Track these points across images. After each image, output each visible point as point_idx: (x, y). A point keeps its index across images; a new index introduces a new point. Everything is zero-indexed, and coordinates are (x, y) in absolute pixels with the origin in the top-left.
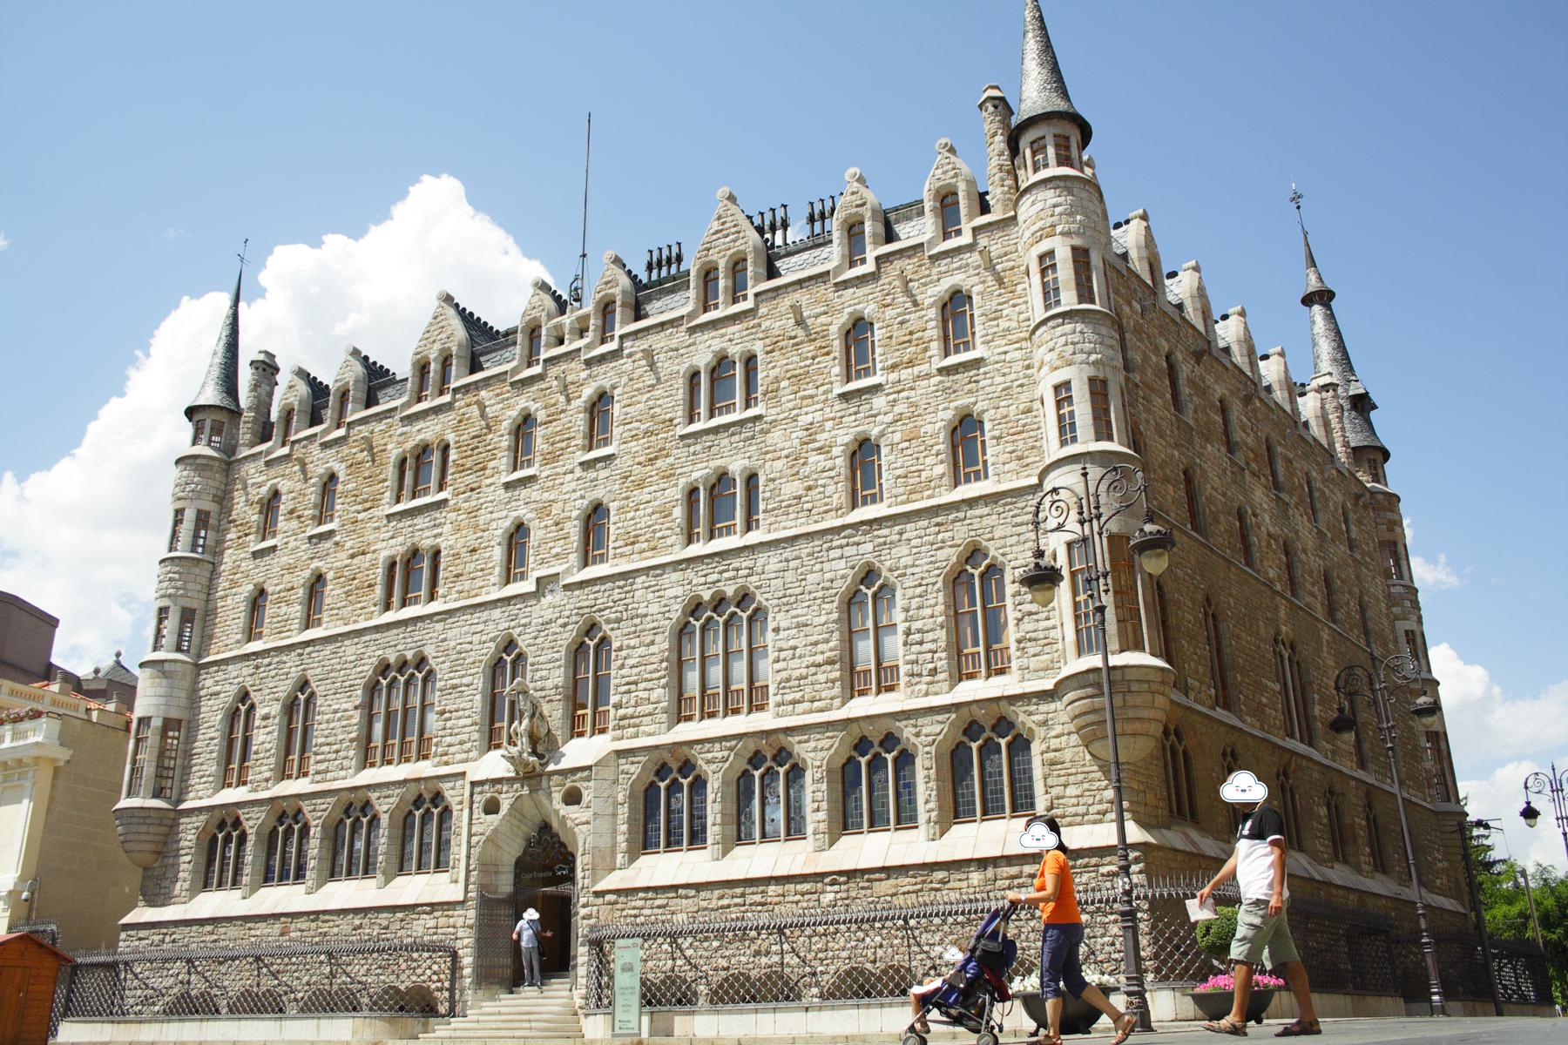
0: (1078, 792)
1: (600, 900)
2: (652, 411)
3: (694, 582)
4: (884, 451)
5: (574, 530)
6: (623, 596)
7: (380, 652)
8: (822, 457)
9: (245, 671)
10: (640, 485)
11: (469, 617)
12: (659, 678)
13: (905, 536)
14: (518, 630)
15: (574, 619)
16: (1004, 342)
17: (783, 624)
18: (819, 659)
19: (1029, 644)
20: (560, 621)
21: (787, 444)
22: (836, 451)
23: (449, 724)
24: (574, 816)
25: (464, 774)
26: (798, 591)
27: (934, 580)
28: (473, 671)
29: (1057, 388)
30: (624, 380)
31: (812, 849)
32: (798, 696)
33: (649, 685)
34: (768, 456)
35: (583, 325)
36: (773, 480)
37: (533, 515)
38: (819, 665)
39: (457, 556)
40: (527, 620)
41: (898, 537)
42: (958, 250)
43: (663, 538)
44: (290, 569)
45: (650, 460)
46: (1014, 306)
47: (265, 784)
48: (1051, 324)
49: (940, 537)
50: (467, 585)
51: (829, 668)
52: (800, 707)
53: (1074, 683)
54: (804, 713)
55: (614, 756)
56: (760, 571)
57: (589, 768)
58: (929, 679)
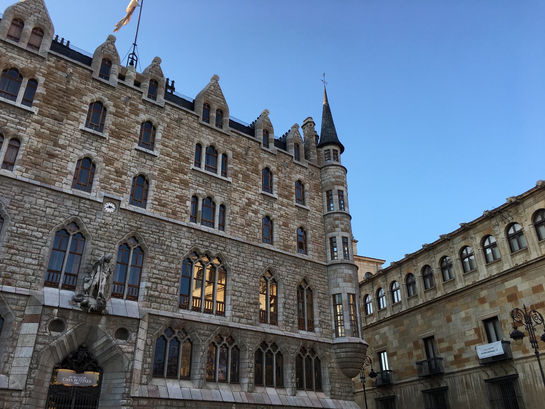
0: (339, 387)
1: (136, 403)
2: (179, 149)
3: (197, 241)
4: (276, 226)
5: (129, 180)
6: (158, 231)
8: (253, 215)
10: (169, 179)
11: (45, 195)
12: (175, 282)
13: (285, 264)
14: (85, 220)
15: (127, 230)
16: (315, 209)
17: (237, 280)
18: (252, 301)
19: (323, 323)
20: (116, 227)
21: (240, 202)
22: (260, 216)
23: (14, 258)
24: (124, 347)
25: (29, 296)
26: (243, 267)
27: (293, 285)
28: (43, 230)
29: (343, 237)
31: (247, 391)
32: (242, 314)
33: (169, 283)
34: (232, 202)
35: (138, 80)
36: (234, 213)
37: (102, 159)
38: (251, 304)
39: (36, 152)
40: (94, 217)
41: (281, 262)
42: (303, 167)
43: (180, 212)
45: (176, 171)
46: (318, 198)
48: (342, 215)
49: (296, 269)
50: (43, 174)
51: (255, 306)
52: (243, 320)
53: (351, 346)
54: (244, 323)
55: (147, 317)
56: (228, 250)
57: (139, 319)
58: (291, 325)
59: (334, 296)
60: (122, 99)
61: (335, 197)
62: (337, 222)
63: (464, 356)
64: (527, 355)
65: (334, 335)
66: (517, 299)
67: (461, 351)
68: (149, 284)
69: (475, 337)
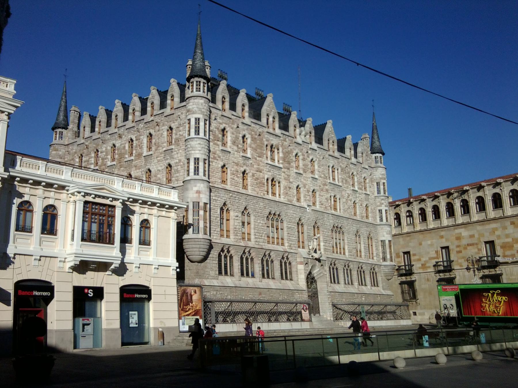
5: (311, 193)
7: (270, 208)
9: (226, 196)
10: (322, 190)
14: (304, 217)
23: (291, 238)
30: (318, 160)
44: (237, 164)
47: (240, 240)
50: (289, 198)
59: (381, 241)
60: (304, 150)
61: (382, 187)
62: (383, 201)
63: (427, 265)
64: (462, 268)
65: (381, 261)
66: (460, 239)
67: (426, 262)
68: (324, 244)
69: (435, 255)
